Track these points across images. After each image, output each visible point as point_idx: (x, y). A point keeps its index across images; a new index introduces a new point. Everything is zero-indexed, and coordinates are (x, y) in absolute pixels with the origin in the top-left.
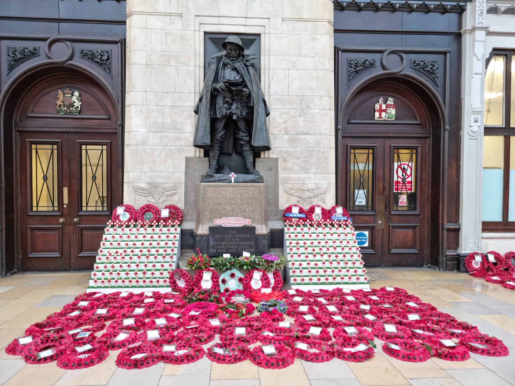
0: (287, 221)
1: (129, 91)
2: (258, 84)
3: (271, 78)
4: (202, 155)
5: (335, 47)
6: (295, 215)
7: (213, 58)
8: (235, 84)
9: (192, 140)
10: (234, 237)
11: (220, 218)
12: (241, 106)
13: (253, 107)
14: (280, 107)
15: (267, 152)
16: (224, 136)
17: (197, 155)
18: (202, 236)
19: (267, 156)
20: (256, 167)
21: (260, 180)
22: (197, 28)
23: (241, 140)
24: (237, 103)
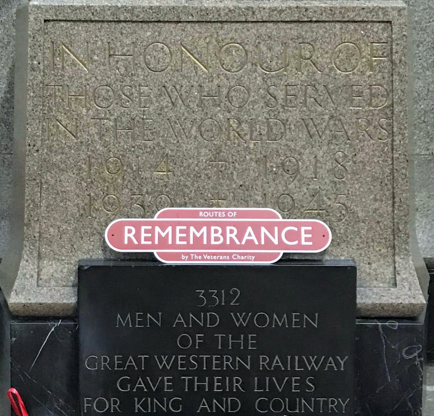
11: (147, 211)
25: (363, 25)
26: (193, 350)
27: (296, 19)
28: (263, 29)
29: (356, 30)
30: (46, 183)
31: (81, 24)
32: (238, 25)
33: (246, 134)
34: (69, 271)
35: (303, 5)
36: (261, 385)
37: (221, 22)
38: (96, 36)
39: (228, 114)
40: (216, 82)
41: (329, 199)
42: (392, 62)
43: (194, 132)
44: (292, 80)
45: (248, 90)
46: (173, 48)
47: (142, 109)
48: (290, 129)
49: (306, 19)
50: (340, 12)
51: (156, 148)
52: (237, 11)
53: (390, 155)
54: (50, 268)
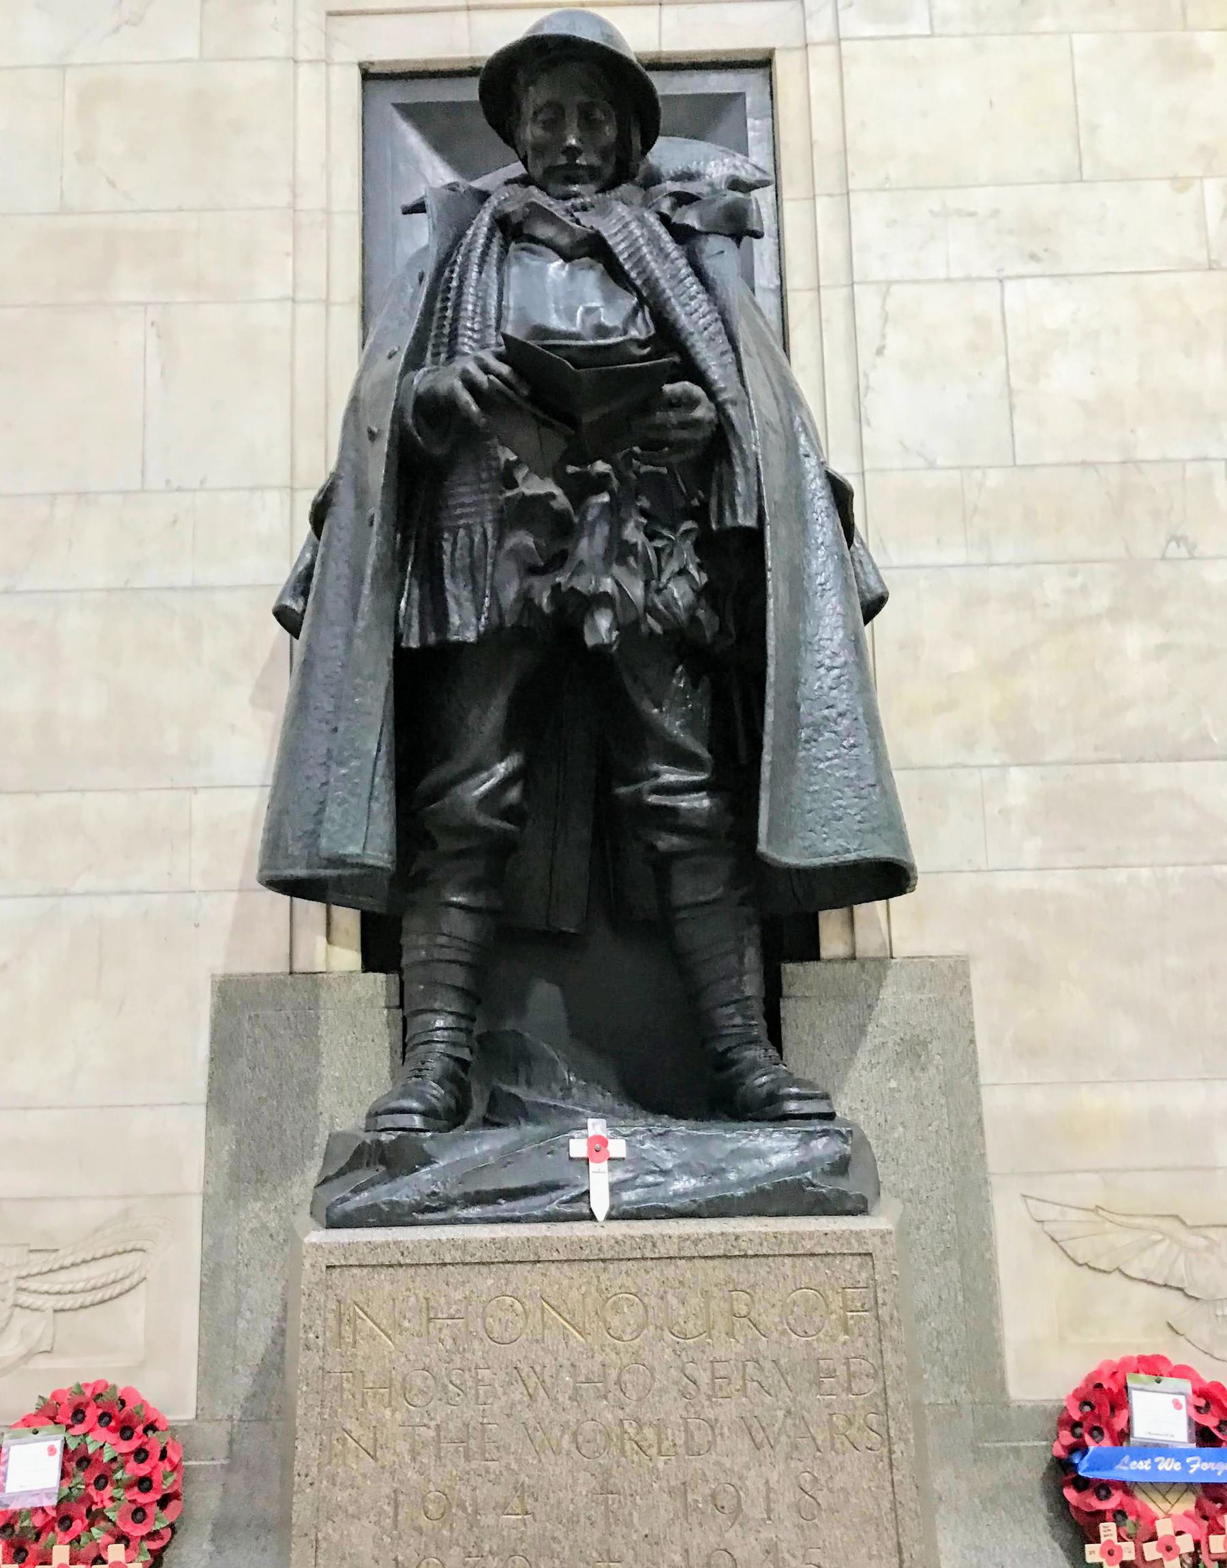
0: (1108, 1530)
2: (781, 366)
6: (1167, 1465)
7: (419, 208)
12: (651, 536)
13: (754, 539)
14: (957, 555)
16: (514, 794)
19: (868, 943)
20: (788, 1034)
23: (668, 819)
25: (827, 1260)
27: (721, 1252)
28: (670, 1271)
29: (817, 1268)
30: (325, 1538)
31: (384, 1271)
32: (630, 1263)
33: (650, 1446)
35: (731, 1230)
37: (604, 1260)
38: (409, 1290)
39: (621, 1412)
40: (599, 1358)
41: (794, 1556)
42: (877, 1318)
43: (566, 1442)
44: (721, 1353)
45: (652, 1370)
46: (529, 1305)
47: (481, 1407)
48: (721, 1434)
49: (737, 1253)
50: (790, 1241)
51: (505, 1473)
52: (628, 1243)
53: (888, 1475)
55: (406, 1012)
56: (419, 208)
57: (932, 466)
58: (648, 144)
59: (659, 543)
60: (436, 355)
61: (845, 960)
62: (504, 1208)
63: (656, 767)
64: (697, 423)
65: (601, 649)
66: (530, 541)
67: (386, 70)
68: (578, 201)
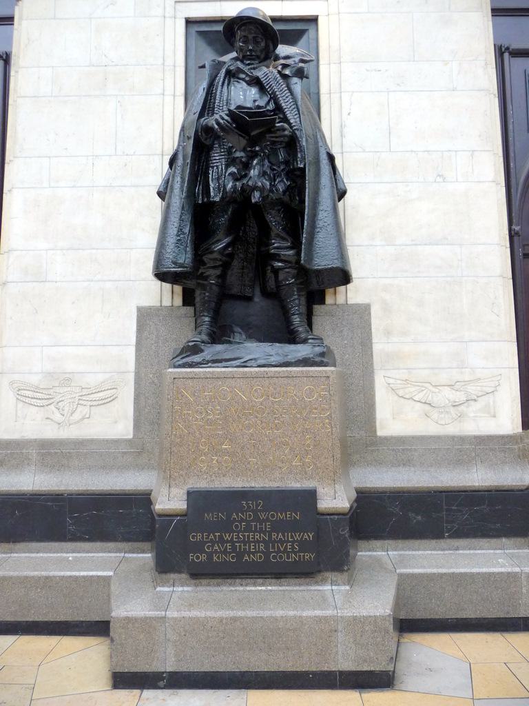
1: (11, 158)
2: (313, 118)
3: (345, 112)
4: (178, 301)
5: (495, 45)
7: (203, 67)
8: (256, 113)
9: (150, 264)
10: (257, 519)
15: (341, 289)
17: (167, 302)
18: (168, 516)
19: (340, 299)
21: (323, 359)
22: (169, 11)
23: (276, 257)
24: (261, 163)
26: (240, 531)
28: (273, 381)
34: (183, 494)
36: (273, 547)
40: (251, 404)
54: (174, 491)
55: (196, 316)
56: (203, 67)
57: (364, 151)
58: (275, 47)
59: (275, 172)
60: (208, 114)
61: (331, 305)
62: (224, 364)
63: (273, 241)
64: (285, 136)
65: (256, 202)
66: (236, 171)
67: (194, 20)
68: (253, 66)
